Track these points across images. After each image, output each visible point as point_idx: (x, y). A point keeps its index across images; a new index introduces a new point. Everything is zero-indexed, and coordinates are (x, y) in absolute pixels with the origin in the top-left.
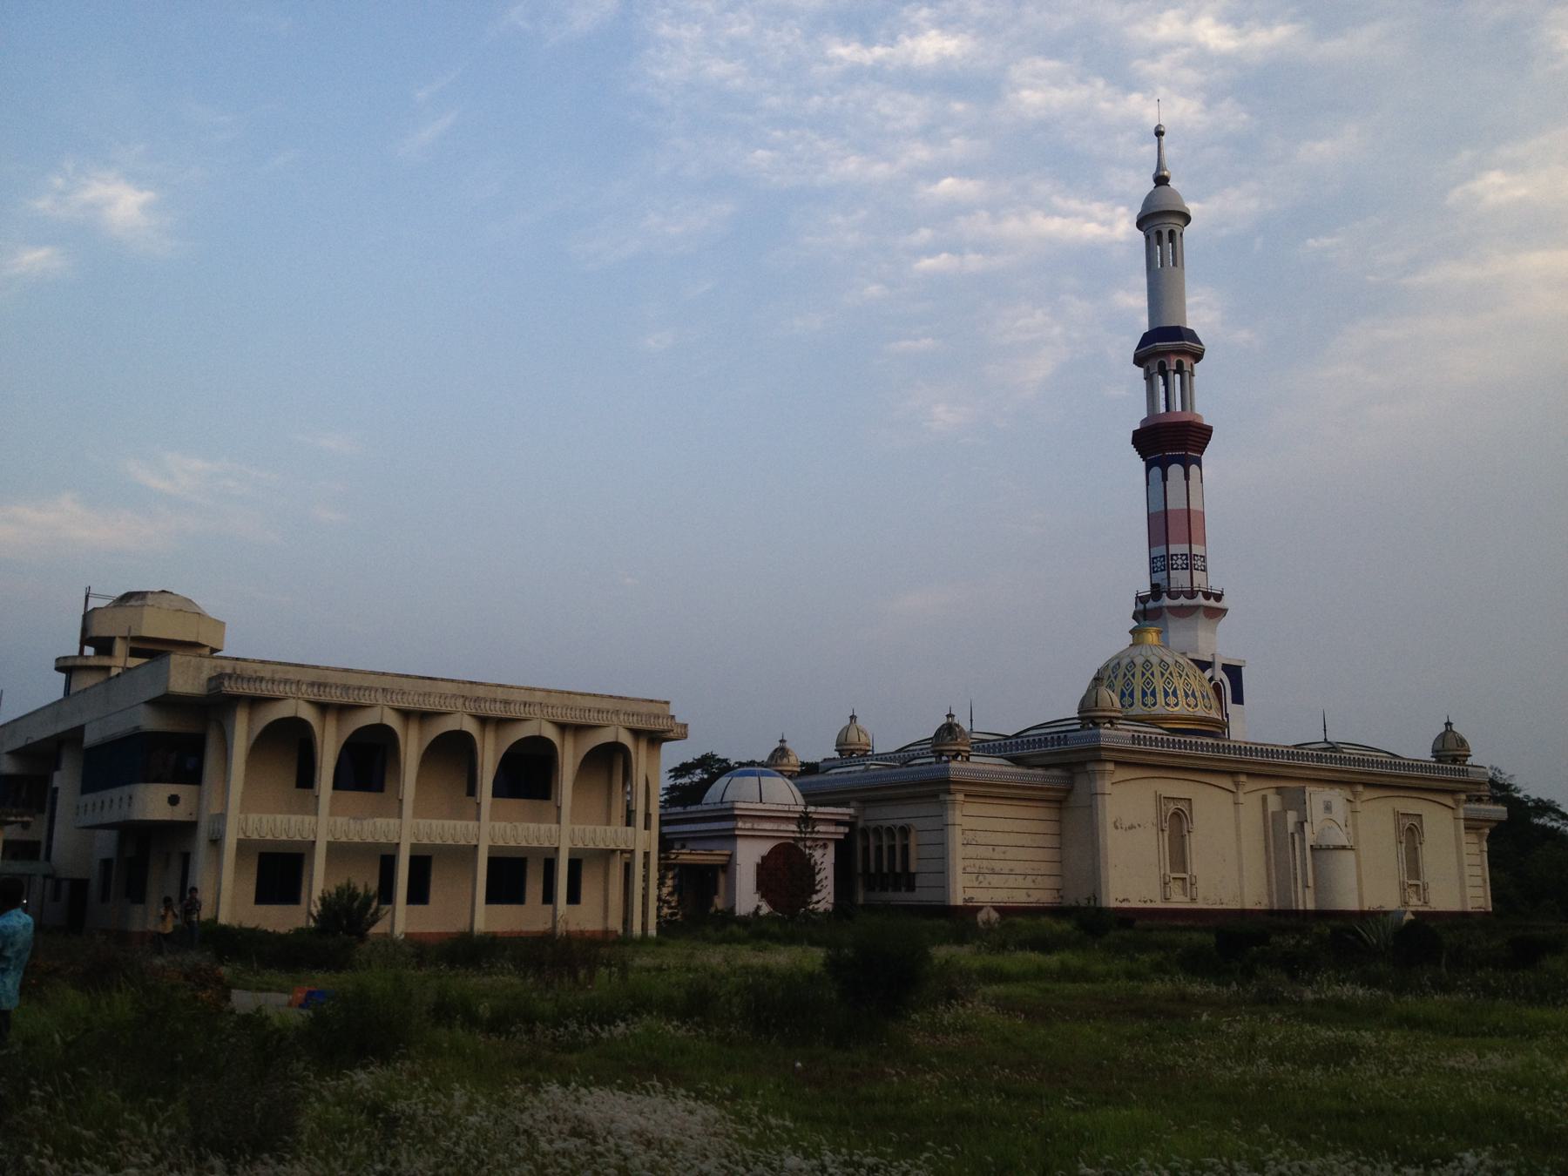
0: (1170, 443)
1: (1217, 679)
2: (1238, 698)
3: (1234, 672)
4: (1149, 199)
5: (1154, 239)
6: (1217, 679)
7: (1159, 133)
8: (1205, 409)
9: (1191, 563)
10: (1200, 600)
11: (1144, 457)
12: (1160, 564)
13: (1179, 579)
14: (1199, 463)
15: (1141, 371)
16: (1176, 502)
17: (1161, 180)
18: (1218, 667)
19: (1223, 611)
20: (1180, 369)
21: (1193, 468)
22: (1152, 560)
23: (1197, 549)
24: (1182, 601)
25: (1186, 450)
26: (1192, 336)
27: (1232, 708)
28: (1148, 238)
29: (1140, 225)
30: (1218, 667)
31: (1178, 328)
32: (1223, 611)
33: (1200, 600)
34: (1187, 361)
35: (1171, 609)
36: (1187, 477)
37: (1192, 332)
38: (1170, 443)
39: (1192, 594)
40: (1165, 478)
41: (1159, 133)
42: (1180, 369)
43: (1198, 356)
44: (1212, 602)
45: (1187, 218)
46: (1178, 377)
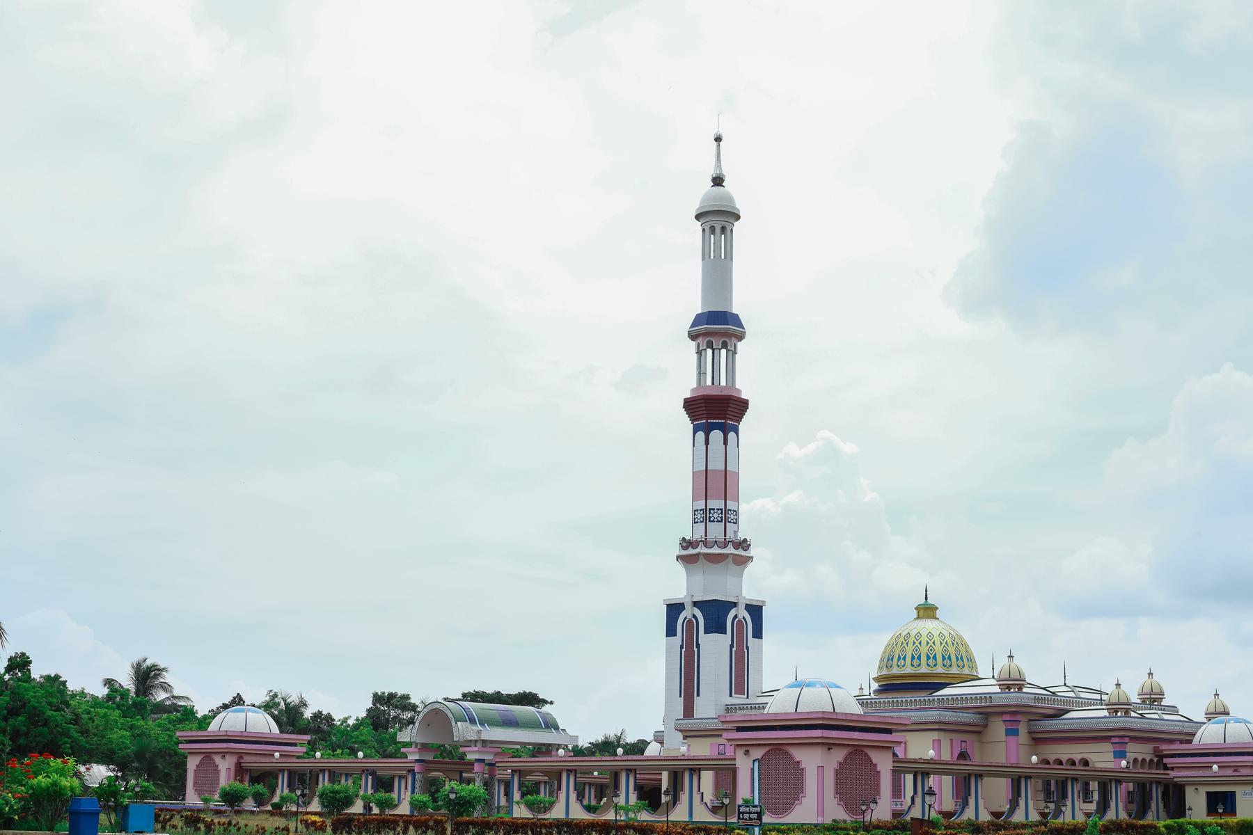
0: (716, 412)
2: (758, 633)
3: (755, 611)
4: (706, 198)
6: (740, 617)
7: (718, 139)
8: (745, 387)
9: (727, 517)
10: (730, 550)
15: (694, 344)
16: (716, 464)
17: (718, 181)
19: (750, 558)
20: (725, 345)
21: (732, 435)
23: (730, 505)
24: (716, 550)
25: (725, 418)
26: (735, 320)
27: (752, 642)
29: (698, 217)
30: (742, 608)
32: (750, 558)
33: (730, 550)
36: (726, 443)
37: (737, 315)
38: (716, 412)
40: (707, 443)
41: (718, 139)
43: (740, 337)
44: (740, 552)
45: (738, 217)
46: (723, 352)
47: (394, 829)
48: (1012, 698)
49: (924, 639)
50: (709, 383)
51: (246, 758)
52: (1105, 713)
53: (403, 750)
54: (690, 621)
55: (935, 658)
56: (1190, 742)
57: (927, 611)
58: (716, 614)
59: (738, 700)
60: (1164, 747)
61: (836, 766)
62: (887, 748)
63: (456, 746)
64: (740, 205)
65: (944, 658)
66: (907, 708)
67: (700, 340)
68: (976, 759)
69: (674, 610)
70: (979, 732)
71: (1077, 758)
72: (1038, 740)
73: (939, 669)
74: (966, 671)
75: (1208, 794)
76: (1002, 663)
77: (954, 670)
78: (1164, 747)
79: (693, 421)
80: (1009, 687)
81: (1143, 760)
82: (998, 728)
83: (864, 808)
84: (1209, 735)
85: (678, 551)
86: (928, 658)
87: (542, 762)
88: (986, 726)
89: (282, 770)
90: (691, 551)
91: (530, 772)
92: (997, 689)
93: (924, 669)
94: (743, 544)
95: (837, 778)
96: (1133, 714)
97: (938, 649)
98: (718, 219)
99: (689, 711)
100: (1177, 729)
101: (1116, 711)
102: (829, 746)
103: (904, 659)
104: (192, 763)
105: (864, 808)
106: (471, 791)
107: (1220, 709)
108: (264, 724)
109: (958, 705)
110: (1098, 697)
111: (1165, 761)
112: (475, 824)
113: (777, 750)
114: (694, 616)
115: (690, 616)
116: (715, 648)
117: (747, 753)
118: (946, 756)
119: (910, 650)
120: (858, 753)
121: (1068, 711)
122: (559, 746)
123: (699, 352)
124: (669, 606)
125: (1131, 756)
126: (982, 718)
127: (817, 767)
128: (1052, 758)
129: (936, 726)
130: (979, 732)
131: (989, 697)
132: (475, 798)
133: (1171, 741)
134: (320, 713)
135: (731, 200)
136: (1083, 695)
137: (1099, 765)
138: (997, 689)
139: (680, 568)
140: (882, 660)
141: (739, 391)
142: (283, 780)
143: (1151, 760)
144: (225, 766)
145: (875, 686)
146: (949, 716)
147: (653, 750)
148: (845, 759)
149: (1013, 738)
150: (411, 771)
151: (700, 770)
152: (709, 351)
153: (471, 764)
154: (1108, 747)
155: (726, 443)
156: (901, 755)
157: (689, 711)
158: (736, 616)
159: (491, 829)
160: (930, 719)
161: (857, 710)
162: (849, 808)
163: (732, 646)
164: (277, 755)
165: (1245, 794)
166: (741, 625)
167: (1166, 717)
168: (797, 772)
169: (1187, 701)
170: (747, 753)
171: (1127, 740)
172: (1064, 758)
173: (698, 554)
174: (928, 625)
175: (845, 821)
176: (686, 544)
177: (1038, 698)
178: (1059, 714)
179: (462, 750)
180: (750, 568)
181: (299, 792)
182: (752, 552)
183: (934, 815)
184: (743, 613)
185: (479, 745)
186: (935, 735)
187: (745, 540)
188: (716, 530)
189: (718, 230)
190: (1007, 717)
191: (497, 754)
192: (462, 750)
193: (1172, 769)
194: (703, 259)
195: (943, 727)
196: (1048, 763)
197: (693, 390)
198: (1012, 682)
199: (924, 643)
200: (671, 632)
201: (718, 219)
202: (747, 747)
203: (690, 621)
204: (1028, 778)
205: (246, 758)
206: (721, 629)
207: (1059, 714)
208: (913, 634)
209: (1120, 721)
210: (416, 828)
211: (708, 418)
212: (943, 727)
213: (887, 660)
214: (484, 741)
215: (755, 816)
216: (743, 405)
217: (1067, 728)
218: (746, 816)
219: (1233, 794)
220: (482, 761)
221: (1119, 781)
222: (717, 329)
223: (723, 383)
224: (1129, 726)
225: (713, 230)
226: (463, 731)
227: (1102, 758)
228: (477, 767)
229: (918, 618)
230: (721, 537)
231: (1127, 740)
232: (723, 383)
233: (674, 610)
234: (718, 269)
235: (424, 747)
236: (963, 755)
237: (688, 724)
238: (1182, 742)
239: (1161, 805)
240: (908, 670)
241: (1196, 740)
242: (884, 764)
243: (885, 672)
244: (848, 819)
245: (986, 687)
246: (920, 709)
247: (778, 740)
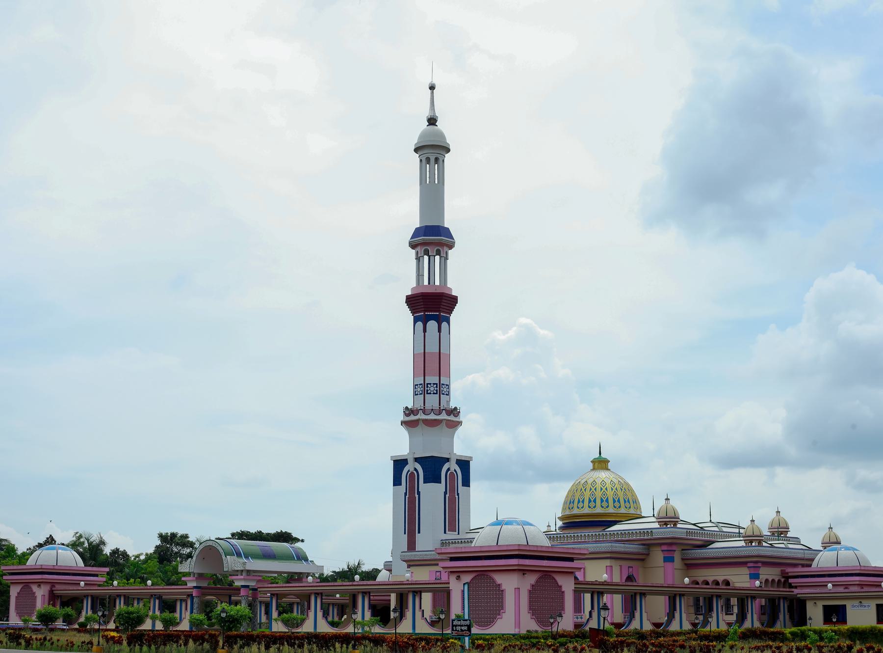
0: (432, 306)
1: (452, 470)
2: (466, 483)
3: (465, 465)
4: (423, 135)
6: (452, 470)
7: (432, 88)
8: (454, 286)
9: (442, 389)
10: (444, 416)
12: (422, 389)
14: (448, 321)
15: (413, 252)
16: (432, 348)
17: (432, 121)
20: (438, 253)
21: (444, 324)
22: (415, 386)
24: (432, 417)
26: (447, 232)
27: (461, 489)
28: (421, 160)
29: (416, 150)
31: (438, 226)
32: (460, 423)
33: (444, 416)
34: (446, 249)
36: (440, 331)
38: (432, 306)
40: (425, 331)
41: (432, 88)
43: (451, 246)
44: (452, 418)
45: (448, 150)
46: (437, 258)
47: (177, 642)
48: (669, 532)
49: (598, 486)
50: (426, 283)
51: (58, 587)
52: (742, 544)
53: (183, 579)
54: (412, 473)
55: (607, 500)
56: (810, 566)
57: (601, 463)
58: (432, 467)
59: (451, 535)
60: (789, 570)
61: (529, 588)
62: (569, 573)
63: (225, 576)
64: (450, 140)
65: (614, 501)
66: (586, 541)
67: (418, 249)
68: (641, 580)
69: (399, 464)
70: (643, 560)
71: (720, 579)
72: (690, 565)
73: (611, 510)
74: (632, 511)
75: (825, 607)
76: (660, 504)
77: (623, 510)
78: (789, 570)
79: (413, 313)
80: (666, 524)
81: (773, 580)
82: (658, 556)
83: (552, 621)
84: (825, 560)
85: (401, 417)
86: (602, 501)
87: (295, 587)
88: (648, 555)
89: (86, 596)
90: (412, 418)
91: (285, 595)
92: (657, 525)
93: (599, 510)
94: (455, 412)
95: (530, 597)
96: (764, 544)
97: (610, 494)
98: (432, 151)
99: (412, 545)
100: (799, 556)
101: (751, 542)
102: (523, 571)
103: (583, 502)
104: (14, 591)
105: (552, 621)
106: (238, 611)
107: (833, 540)
108: (72, 559)
109: (626, 538)
110: (737, 530)
111: (791, 581)
112: (241, 637)
113: (482, 575)
114: (415, 469)
115: (412, 470)
116: (432, 495)
117: (458, 578)
118: (616, 579)
119: (587, 495)
120: (546, 576)
121: (713, 542)
122: (308, 574)
123: (418, 259)
124: (395, 461)
125: (763, 577)
126: (646, 547)
127: (514, 588)
128: (700, 580)
129: (609, 555)
130: (643, 560)
131: (650, 531)
132: (241, 616)
133: (795, 565)
134: (117, 550)
135: (442, 136)
136: (725, 529)
137: (737, 585)
138: (657, 525)
139: (404, 433)
140: (565, 503)
141: (450, 289)
142: (87, 604)
143: (779, 581)
144: (40, 593)
145: (560, 523)
146: (620, 547)
147: (383, 576)
148: (537, 582)
149: (669, 564)
150: (190, 596)
151: (421, 592)
152: (426, 258)
153: (238, 589)
154: (745, 571)
155: (440, 331)
156: (581, 579)
157: (412, 545)
158: (449, 469)
159: (255, 641)
160: (603, 550)
161: (546, 543)
162: (540, 621)
163: (445, 493)
164: (82, 583)
165: (853, 606)
166: (452, 477)
167: (790, 546)
168: (499, 593)
169: (807, 532)
170: (458, 578)
171: (760, 565)
172: (710, 579)
173: (418, 420)
174: (602, 475)
175: (536, 631)
176: (408, 412)
177: (689, 532)
178: (705, 545)
179: (230, 578)
180: (460, 432)
181: (100, 614)
182: (462, 417)
183: (607, 626)
184: (454, 467)
185: (244, 574)
186: (608, 562)
187: (456, 408)
188: (432, 401)
190: (665, 548)
191: (259, 581)
192: (230, 578)
193: (796, 587)
194: (421, 184)
195: (615, 556)
196: (698, 583)
197: (412, 289)
198: (669, 519)
199: (598, 489)
200: (397, 482)
201: (432, 151)
202: (458, 573)
203: (412, 473)
204: (681, 595)
205: (58, 587)
206: (438, 480)
207: (705, 545)
208: (590, 482)
209: (754, 550)
210: (195, 641)
211: (425, 311)
212: (615, 556)
213: (569, 502)
214: (248, 571)
215: (466, 628)
217: (711, 555)
218: (459, 628)
219: (845, 606)
220: (247, 586)
221: (753, 598)
222: (432, 239)
223: (437, 283)
224: (762, 553)
225: (428, 160)
226: (231, 563)
227: (740, 579)
228: (243, 592)
229: (594, 469)
230: (436, 406)
231: (760, 565)
232: (437, 283)
233: (399, 464)
234: (432, 194)
235: (200, 576)
236: (630, 578)
237: (411, 555)
238: (803, 566)
239: (787, 617)
240: (586, 510)
241: (814, 564)
242: (567, 586)
243: (568, 513)
244: (539, 629)
245: (648, 523)
246: (596, 542)
247: (483, 567)
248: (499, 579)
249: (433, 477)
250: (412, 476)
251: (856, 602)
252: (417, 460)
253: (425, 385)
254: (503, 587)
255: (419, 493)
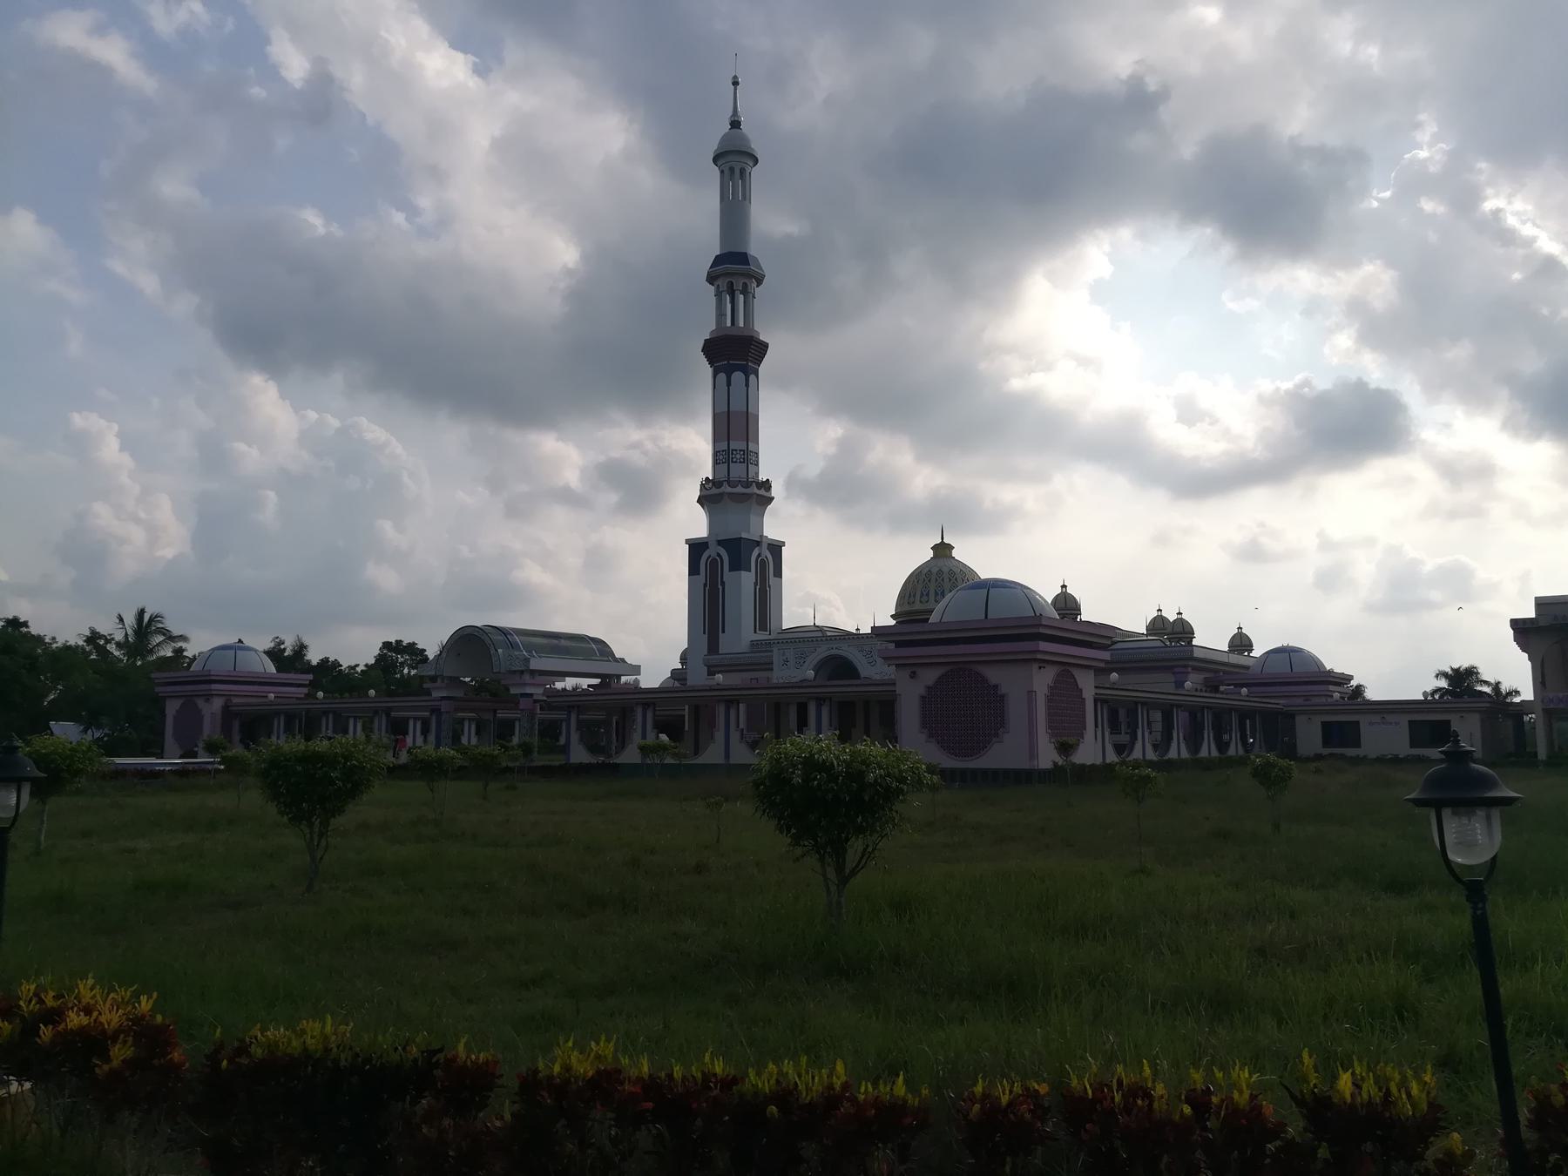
3: (776, 548)
5: (727, 171)
11: (711, 363)
13: (737, 471)
16: (737, 405)
17: (735, 124)
18: (765, 546)
21: (752, 377)
24: (739, 489)
27: (772, 580)
29: (715, 160)
35: (730, 494)
36: (747, 385)
39: (747, 484)
40: (729, 384)
41: (735, 83)
42: (745, 291)
43: (759, 282)
44: (762, 492)
45: (756, 161)
67: (719, 282)
99: (713, 646)
115: (714, 555)
123: (718, 294)
150: (436, 711)
165: (1371, 724)
170: (913, 675)
182: (774, 492)
188: (737, 471)
189: (737, 172)
200: (693, 569)
216: (764, 347)
234: (734, 212)
237: (715, 659)
248: (993, 675)
249: (738, 564)
250: (714, 565)
251: (1376, 718)
252: (720, 543)
253: (729, 452)
254: (1003, 690)
255: (723, 584)
